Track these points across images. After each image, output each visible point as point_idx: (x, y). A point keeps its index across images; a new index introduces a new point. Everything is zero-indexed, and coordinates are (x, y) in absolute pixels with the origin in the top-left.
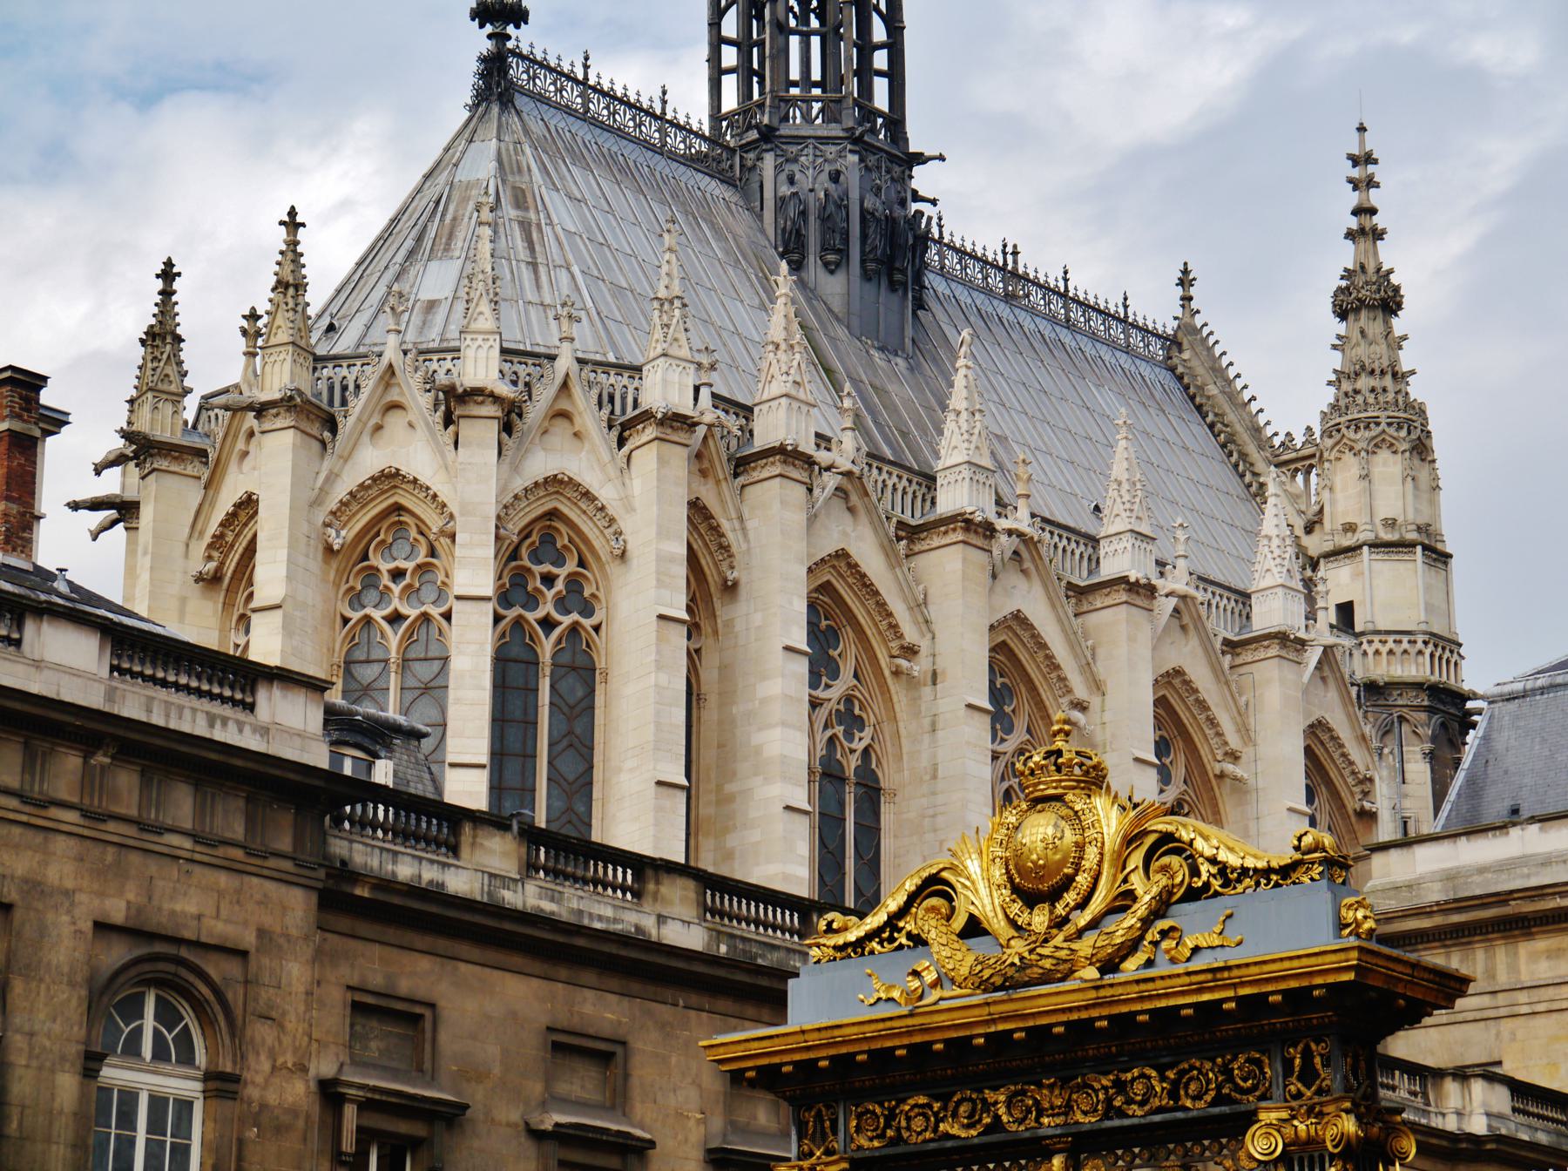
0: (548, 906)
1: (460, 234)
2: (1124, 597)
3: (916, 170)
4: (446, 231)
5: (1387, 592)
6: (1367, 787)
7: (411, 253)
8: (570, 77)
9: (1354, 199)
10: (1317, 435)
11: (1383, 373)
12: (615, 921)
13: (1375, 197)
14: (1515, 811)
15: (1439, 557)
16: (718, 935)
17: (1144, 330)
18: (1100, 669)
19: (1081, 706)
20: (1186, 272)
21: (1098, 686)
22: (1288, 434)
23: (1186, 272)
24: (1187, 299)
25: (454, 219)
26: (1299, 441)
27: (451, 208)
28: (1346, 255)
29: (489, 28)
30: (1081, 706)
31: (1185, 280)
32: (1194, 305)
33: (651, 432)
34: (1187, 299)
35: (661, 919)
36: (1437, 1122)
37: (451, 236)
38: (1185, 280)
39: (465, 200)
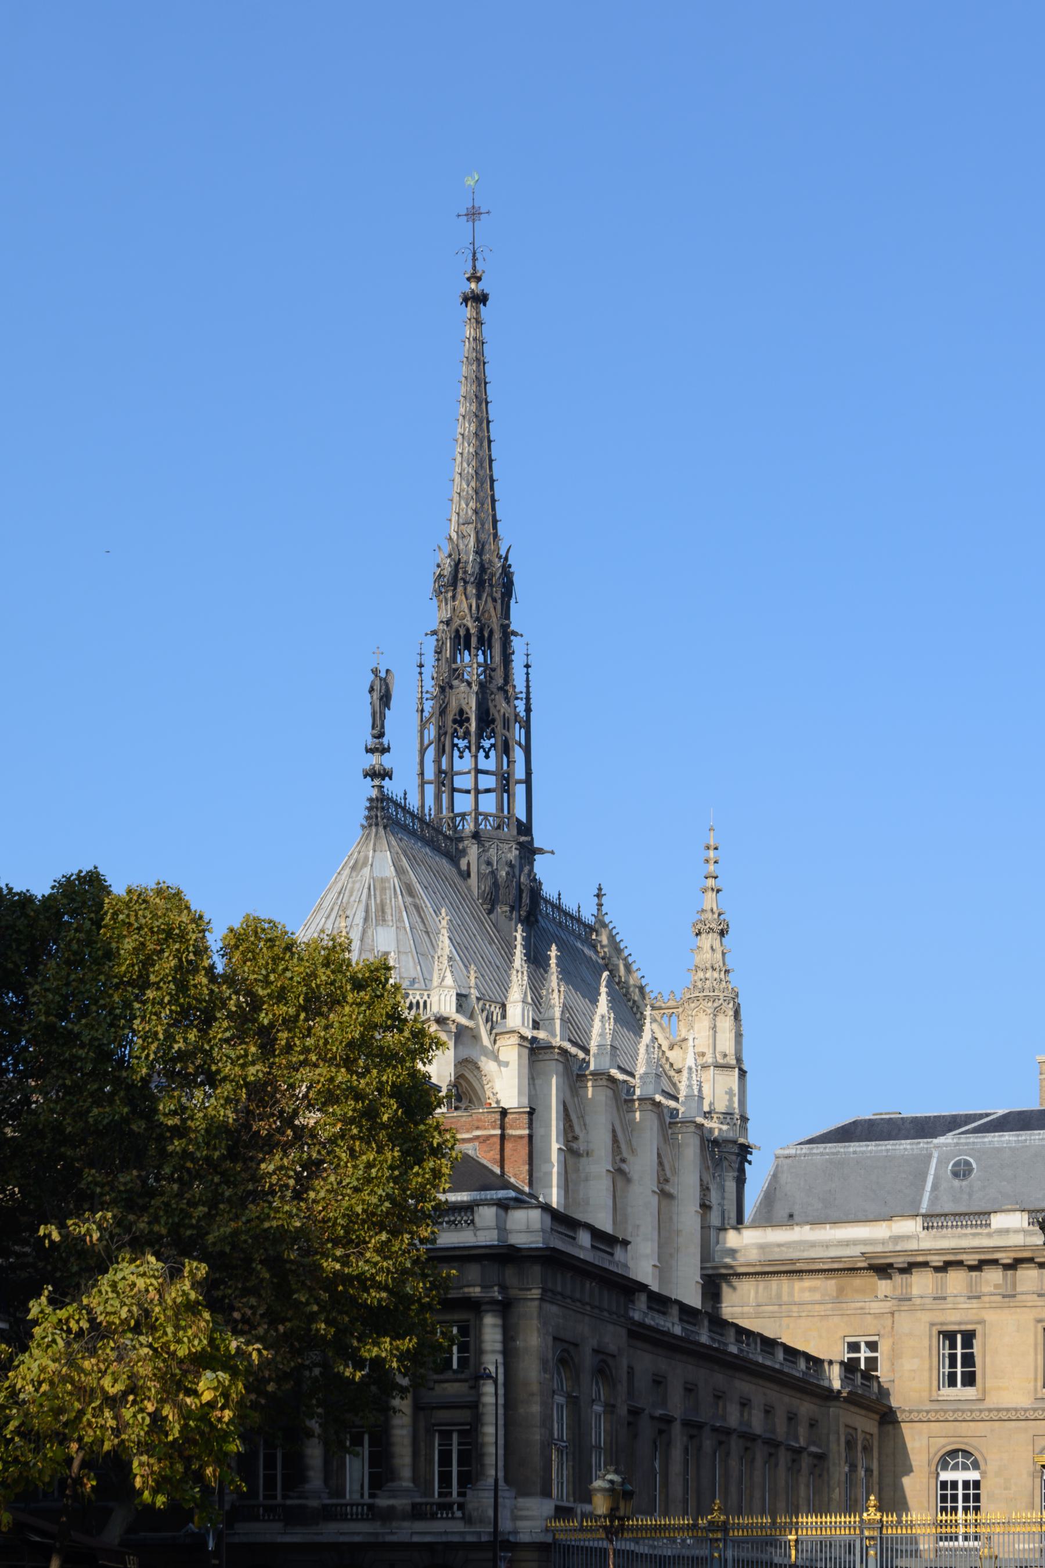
0: (652, 1323)
1: (388, 911)
2: (650, 1108)
4: (380, 908)
6: (706, 1192)
7: (366, 920)
8: (401, 807)
12: (664, 1326)
14: (791, 1216)
16: (683, 1329)
18: (634, 1143)
21: (633, 1151)
25: (382, 901)
27: (378, 893)
35: (673, 1324)
36: (821, 1383)
37: (383, 912)
39: (383, 890)
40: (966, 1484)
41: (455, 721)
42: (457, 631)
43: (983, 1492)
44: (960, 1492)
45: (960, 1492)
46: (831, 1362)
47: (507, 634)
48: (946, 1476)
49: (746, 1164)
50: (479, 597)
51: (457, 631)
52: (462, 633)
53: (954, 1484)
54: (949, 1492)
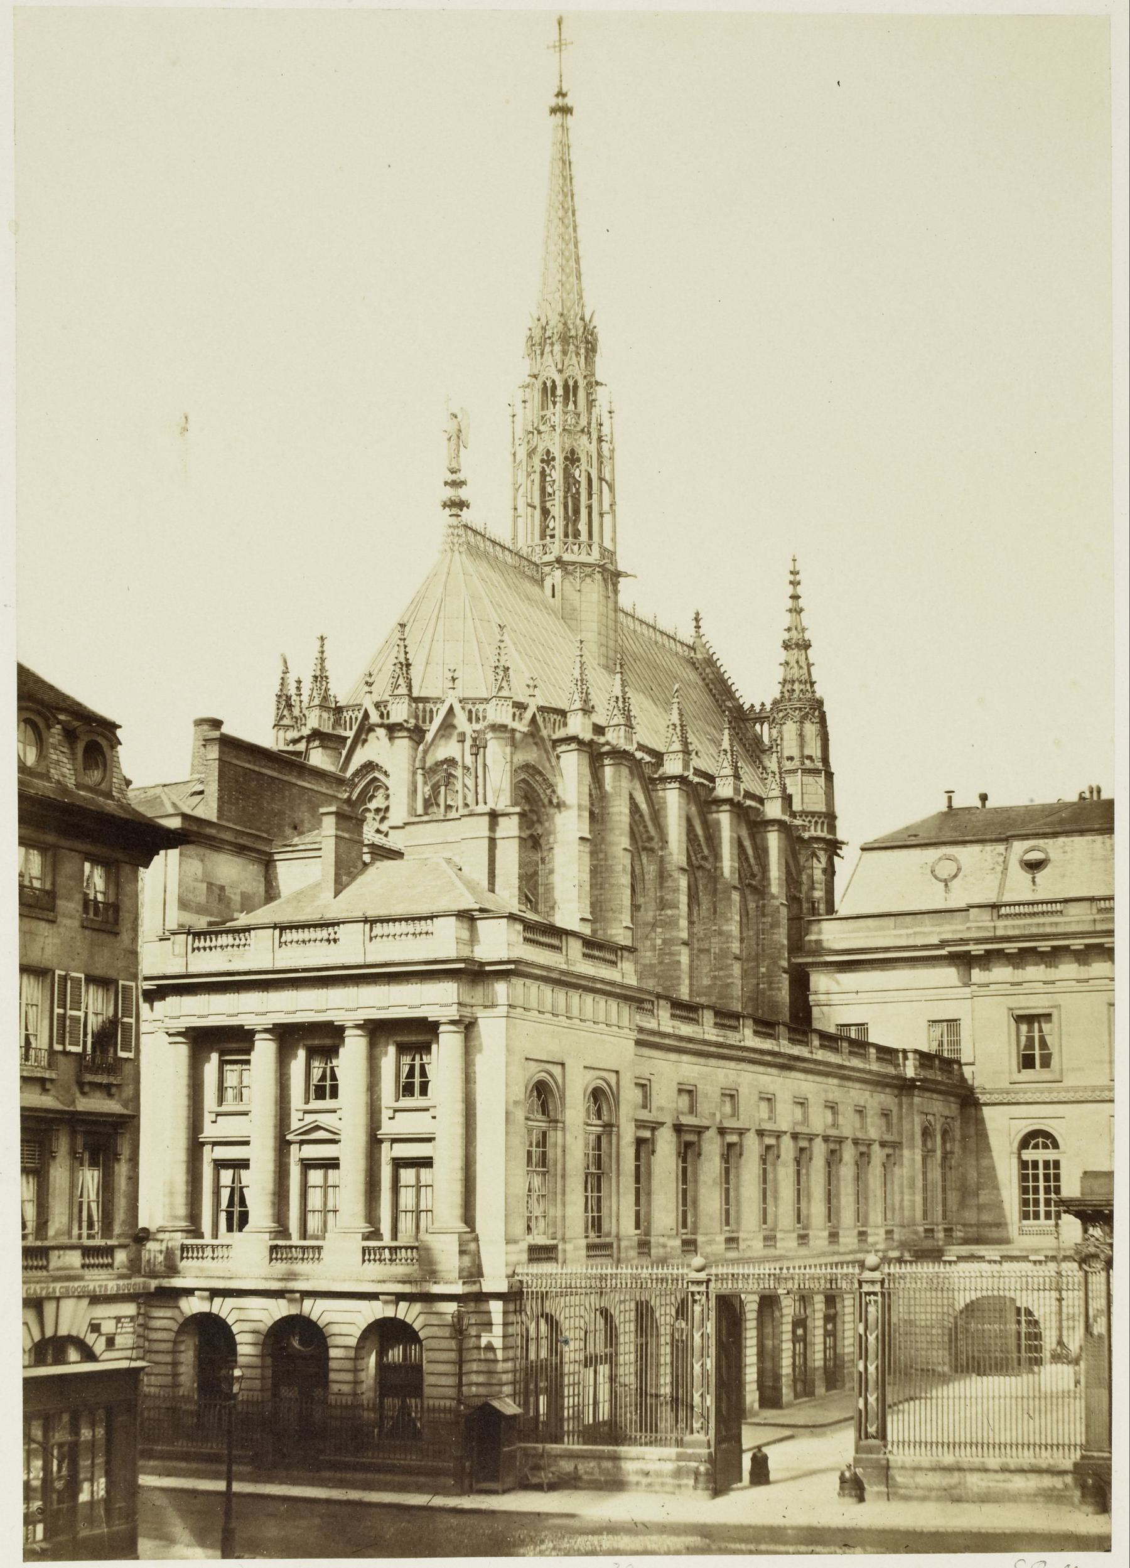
3: (620, 579)
5: (807, 794)
8: (480, 534)
9: (790, 590)
10: (768, 707)
11: (806, 682)
13: (800, 590)
15: (829, 776)
17: (682, 643)
19: (705, 858)
20: (697, 614)
22: (752, 706)
23: (697, 614)
24: (698, 627)
26: (758, 708)
28: (787, 620)
29: (447, 511)
30: (705, 858)
31: (697, 620)
32: (702, 631)
33: (574, 746)
34: (698, 627)
38: (697, 620)
40: (1047, 1164)
41: (542, 461)
42: (545, 383)
43: (1063, 1172)
44: (1041, 1171)
45: (1041, 1171)
46: (905, 1052)
47: (593, 384)
48: (1029, 1155)
49: (836, 858)
50: (565, 353)
51: (545, 383)
52: (549, 384)
53: (1035, 1164)
54: (1030, 1172)
